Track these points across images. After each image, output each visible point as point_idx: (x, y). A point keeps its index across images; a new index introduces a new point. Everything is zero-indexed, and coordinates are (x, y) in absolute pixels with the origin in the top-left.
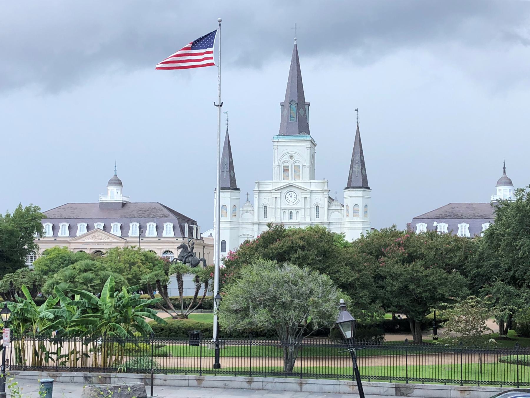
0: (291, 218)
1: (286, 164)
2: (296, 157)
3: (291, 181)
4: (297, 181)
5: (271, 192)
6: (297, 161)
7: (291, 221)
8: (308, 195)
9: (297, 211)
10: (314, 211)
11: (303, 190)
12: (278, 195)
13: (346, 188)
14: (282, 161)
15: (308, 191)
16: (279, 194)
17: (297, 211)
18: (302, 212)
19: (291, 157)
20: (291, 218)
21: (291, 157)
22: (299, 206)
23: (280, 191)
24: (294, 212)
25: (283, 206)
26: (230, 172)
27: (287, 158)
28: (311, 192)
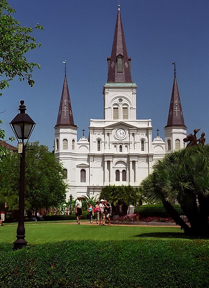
0: (121, 150)
2: (124, 101)
3: (121, 120)
4: (127, 120)
5: (103, 129)
7: (121, 153)
9: (127, 144)
13: (166, 127)
17: (127, 144)
19: (121, 100)
20: (121, 150)
21: (121, 100)
22: (127, 140)
24: (124, 146)
26: (69, 111)
27: (117, 101)
28: (138, 129)
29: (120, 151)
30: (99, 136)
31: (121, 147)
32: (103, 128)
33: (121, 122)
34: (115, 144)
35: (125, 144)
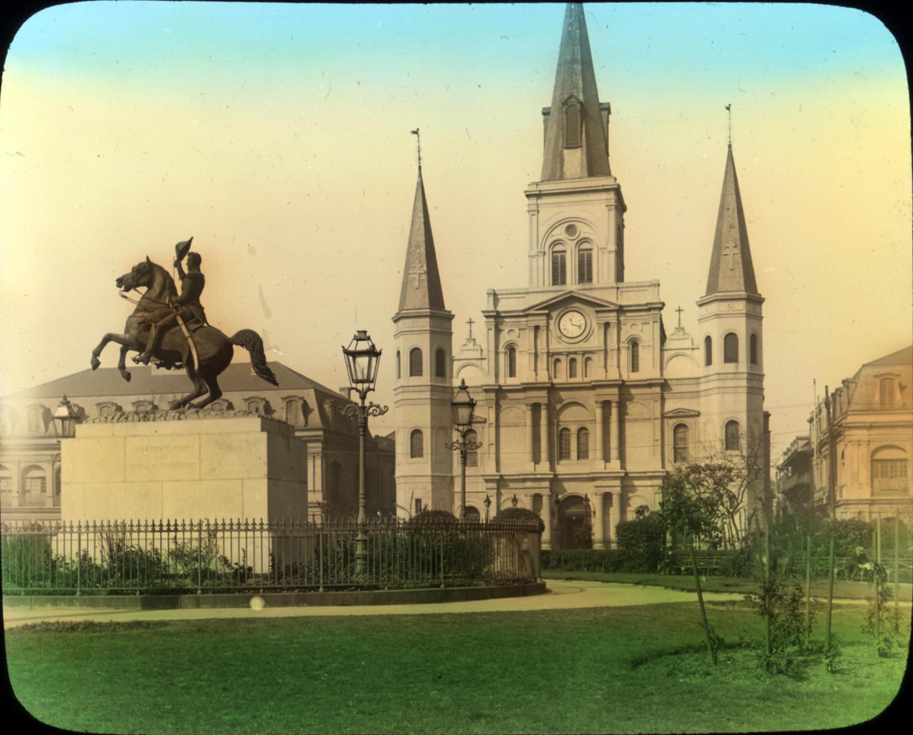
0: (572, 374)
1: (558, 248)
3: (572, 284)
6: (585, 240)
8: (612, 318)
9: (587, 356)
10: (625, 356)
11: (598, 307)
12: (541, 321)
14: (550, 240)
15: (612, 307)
16: (545, 318)
17: (587, 356)
18: (598, 359)
20: (572, 374)
23: (546, 311)
24: (579, 359)
25: (555, 346)
27: (560, 233)
28: (621, 310)
29: (571, 377)
30: (512, 337)
31: (573, 361)
32: (524, 311)
33: (571, 292)
34: (554, 358)
35: (584, 353)
